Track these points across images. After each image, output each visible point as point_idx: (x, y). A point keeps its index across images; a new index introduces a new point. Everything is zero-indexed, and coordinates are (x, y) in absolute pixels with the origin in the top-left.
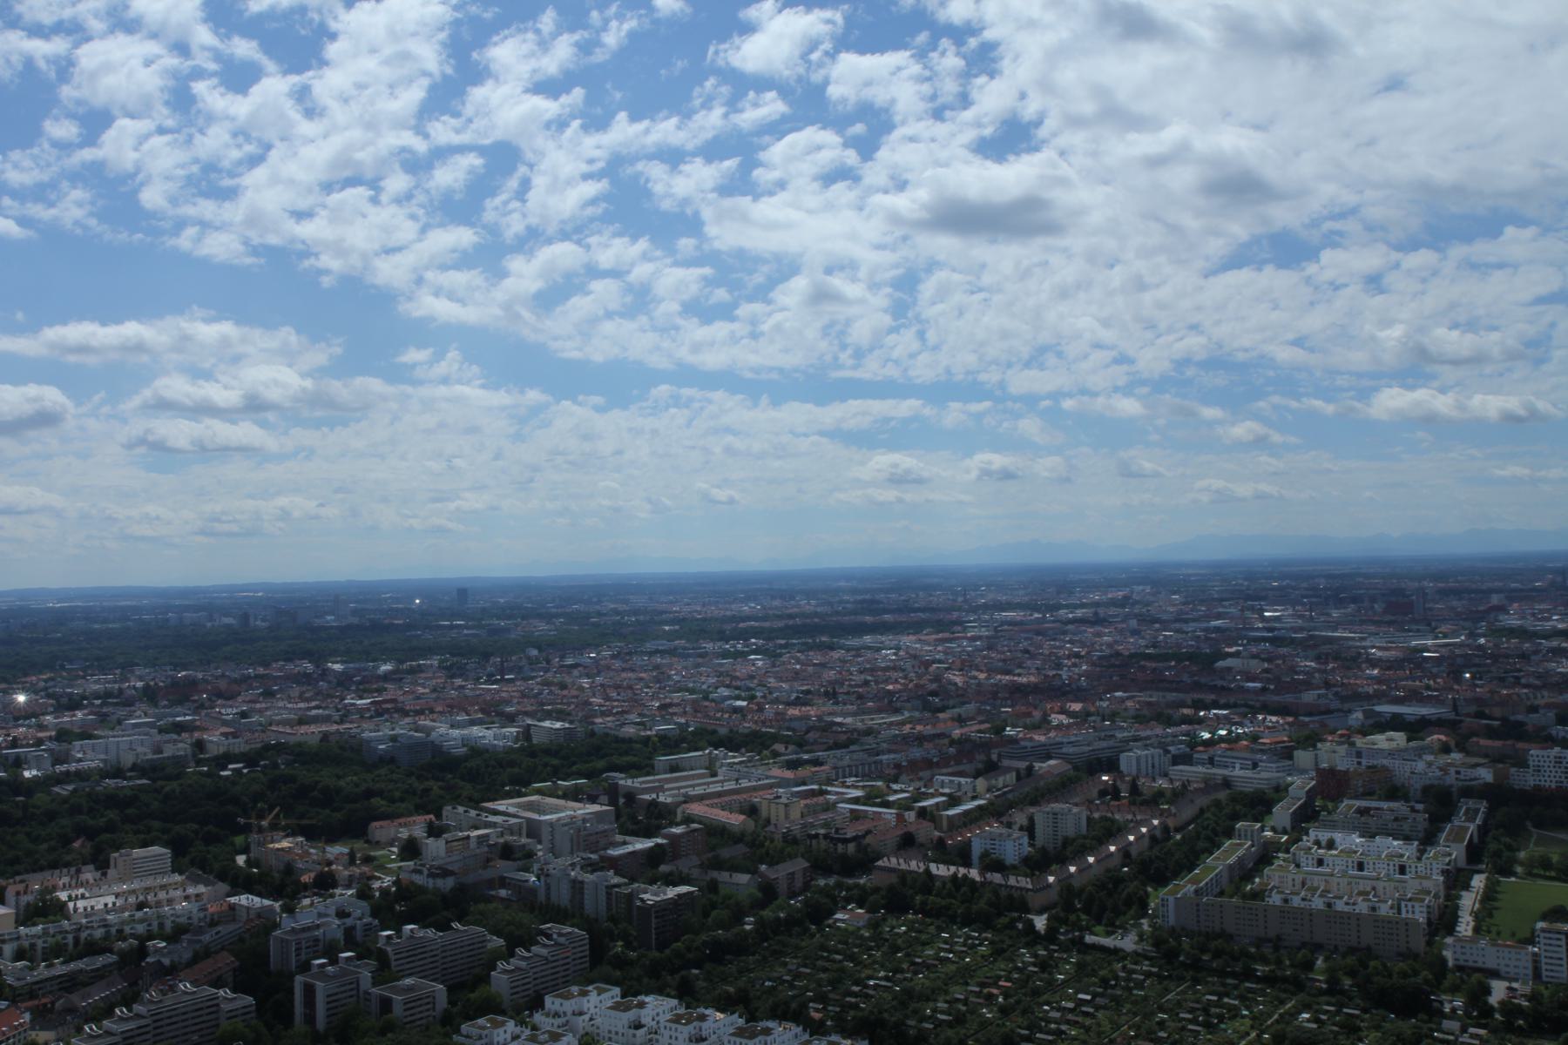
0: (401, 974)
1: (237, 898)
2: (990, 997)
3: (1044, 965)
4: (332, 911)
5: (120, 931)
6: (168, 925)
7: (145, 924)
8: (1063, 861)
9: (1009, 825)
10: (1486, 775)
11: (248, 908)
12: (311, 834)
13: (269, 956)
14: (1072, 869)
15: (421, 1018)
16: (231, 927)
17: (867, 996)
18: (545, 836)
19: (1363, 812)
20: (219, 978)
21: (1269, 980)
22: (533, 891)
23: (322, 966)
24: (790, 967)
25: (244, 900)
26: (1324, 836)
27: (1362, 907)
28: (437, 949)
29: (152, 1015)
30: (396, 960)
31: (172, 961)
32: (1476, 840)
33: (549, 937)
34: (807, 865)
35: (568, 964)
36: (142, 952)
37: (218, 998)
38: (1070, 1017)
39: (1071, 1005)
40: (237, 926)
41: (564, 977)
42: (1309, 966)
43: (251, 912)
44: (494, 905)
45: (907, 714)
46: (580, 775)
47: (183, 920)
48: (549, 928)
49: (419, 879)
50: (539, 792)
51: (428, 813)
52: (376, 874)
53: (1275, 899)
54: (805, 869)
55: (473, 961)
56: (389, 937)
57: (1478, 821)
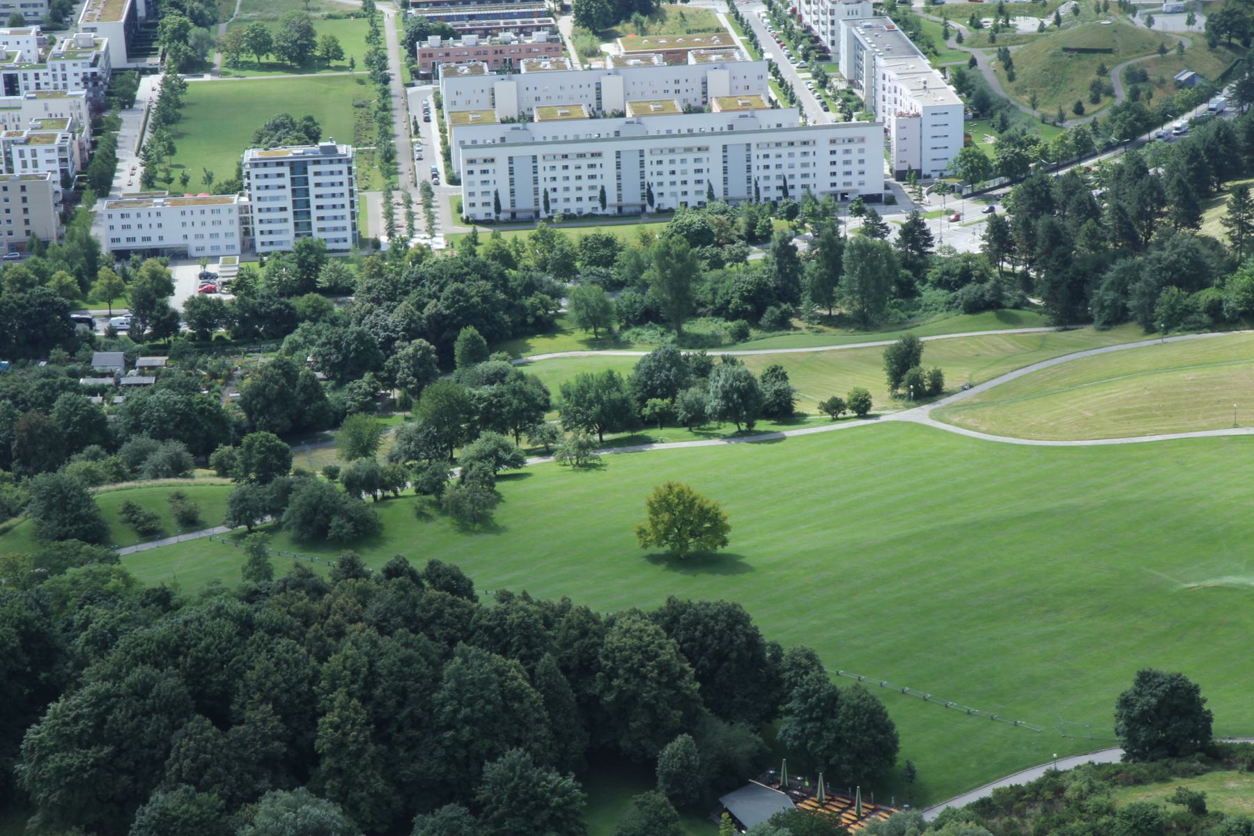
32: (142, 12)
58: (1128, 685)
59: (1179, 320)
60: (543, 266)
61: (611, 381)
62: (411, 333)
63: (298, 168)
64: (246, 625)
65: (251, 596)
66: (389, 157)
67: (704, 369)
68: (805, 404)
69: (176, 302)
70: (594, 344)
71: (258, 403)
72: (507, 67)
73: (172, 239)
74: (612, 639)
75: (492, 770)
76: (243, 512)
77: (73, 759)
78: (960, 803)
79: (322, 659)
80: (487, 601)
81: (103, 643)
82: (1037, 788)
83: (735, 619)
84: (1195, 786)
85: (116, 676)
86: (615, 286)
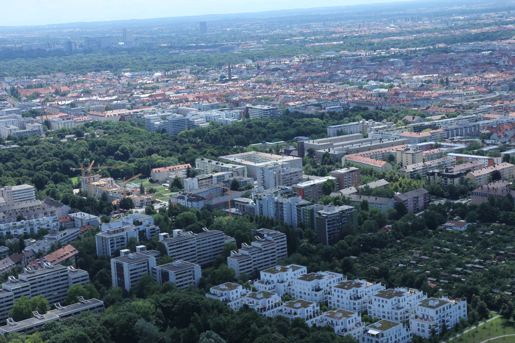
0: (174, 258)
1: (75, 214)
4: (131, 221)
5: (8, 233)
6: (36, 230)
7: (23, 229)
11: (82, 220)
12: (116, 175)
13: (96, 248)
15: (187, 284)
16: (73, 231)
17: (466, 274)
18: (259, 176)
20: (67, 260)
22: (252, 209)
23: (126, 253)
24: (415, 255)
25: (79, 215)
28: (195, 243)
29: (29, 281)
30: (170, 250)
31: (39, 250)
33: (262, 236)
35: (274, 252)
36: (22, 246)
37: (66, 271)
40: (76, 230)
41: (272, 260)
43: (84, 222)
44: (227, 218)
45: (498, 94)
46: (280, 138)
47: (45, 227)
48: (262, 231)
49: (182, 202)
50: (255, 149)
51: (187, 163)
52: (157, 199)
55: (217, 251)
56: (165, 236)
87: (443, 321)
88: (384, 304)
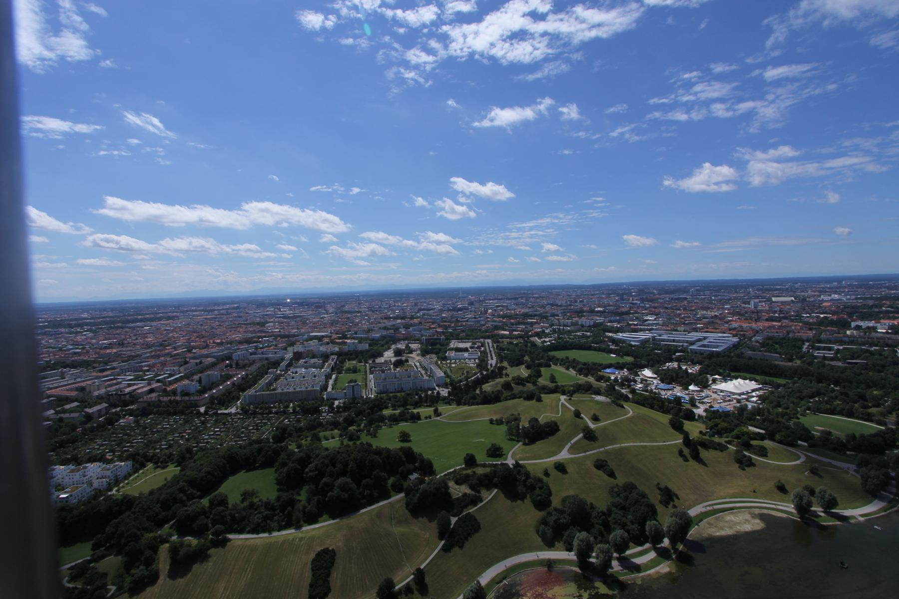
2: (183, 436)
3: (203, 423)
8: (211, 389)
9: (192, 381)
10: (337, 349)
14: (214, 391)
17: (133, 446)
19: (306, 362)
21: (276, 413)
24: (98, 443)
26: (294, 370)
27: (304, 389)
34: (107, 405)
38: (212, 437)
39: (212, 433)
42: (288, 406)
53: (279, 391)
54: (106, 407)
57: (335, 361)
58: (465, 456)
59: (473, 404)
60: (387, 399)
61: (395, 414)
62: (368, 409)
63: (353, 386)
64: (338, 452)
65: (340, 448)
66: (366, 384)
67: (408, 413)
68: (422, 417)
69: (335, 406)
70: (393, 410)
71: (345, 420)
72: (383, 371)
73: (335, 397)
74: (392, 452)
75: (374, 473)
76: (341, 436)
77: (311, 474)
78: (442, 475)
79: (350, 456)
80: (374, 447)
81: (317, 456)
82: (453, 471)
83: (410, 449)
84: (474, 470)
85: (319, 461)
86: (397, 402)
87: (116, 476)
88: (74, 477)
